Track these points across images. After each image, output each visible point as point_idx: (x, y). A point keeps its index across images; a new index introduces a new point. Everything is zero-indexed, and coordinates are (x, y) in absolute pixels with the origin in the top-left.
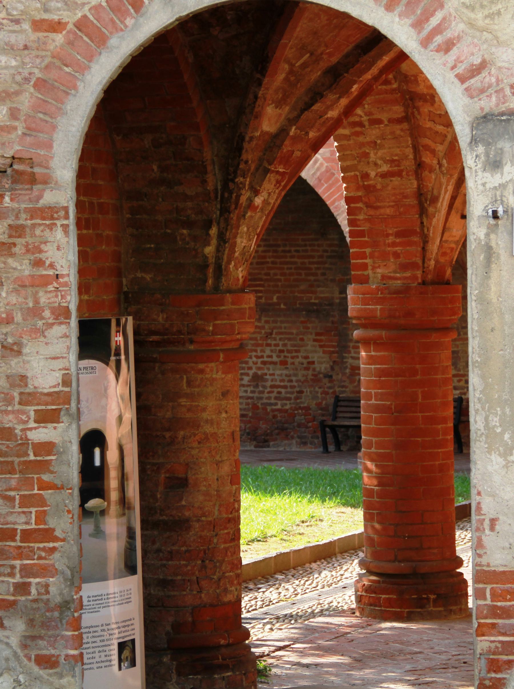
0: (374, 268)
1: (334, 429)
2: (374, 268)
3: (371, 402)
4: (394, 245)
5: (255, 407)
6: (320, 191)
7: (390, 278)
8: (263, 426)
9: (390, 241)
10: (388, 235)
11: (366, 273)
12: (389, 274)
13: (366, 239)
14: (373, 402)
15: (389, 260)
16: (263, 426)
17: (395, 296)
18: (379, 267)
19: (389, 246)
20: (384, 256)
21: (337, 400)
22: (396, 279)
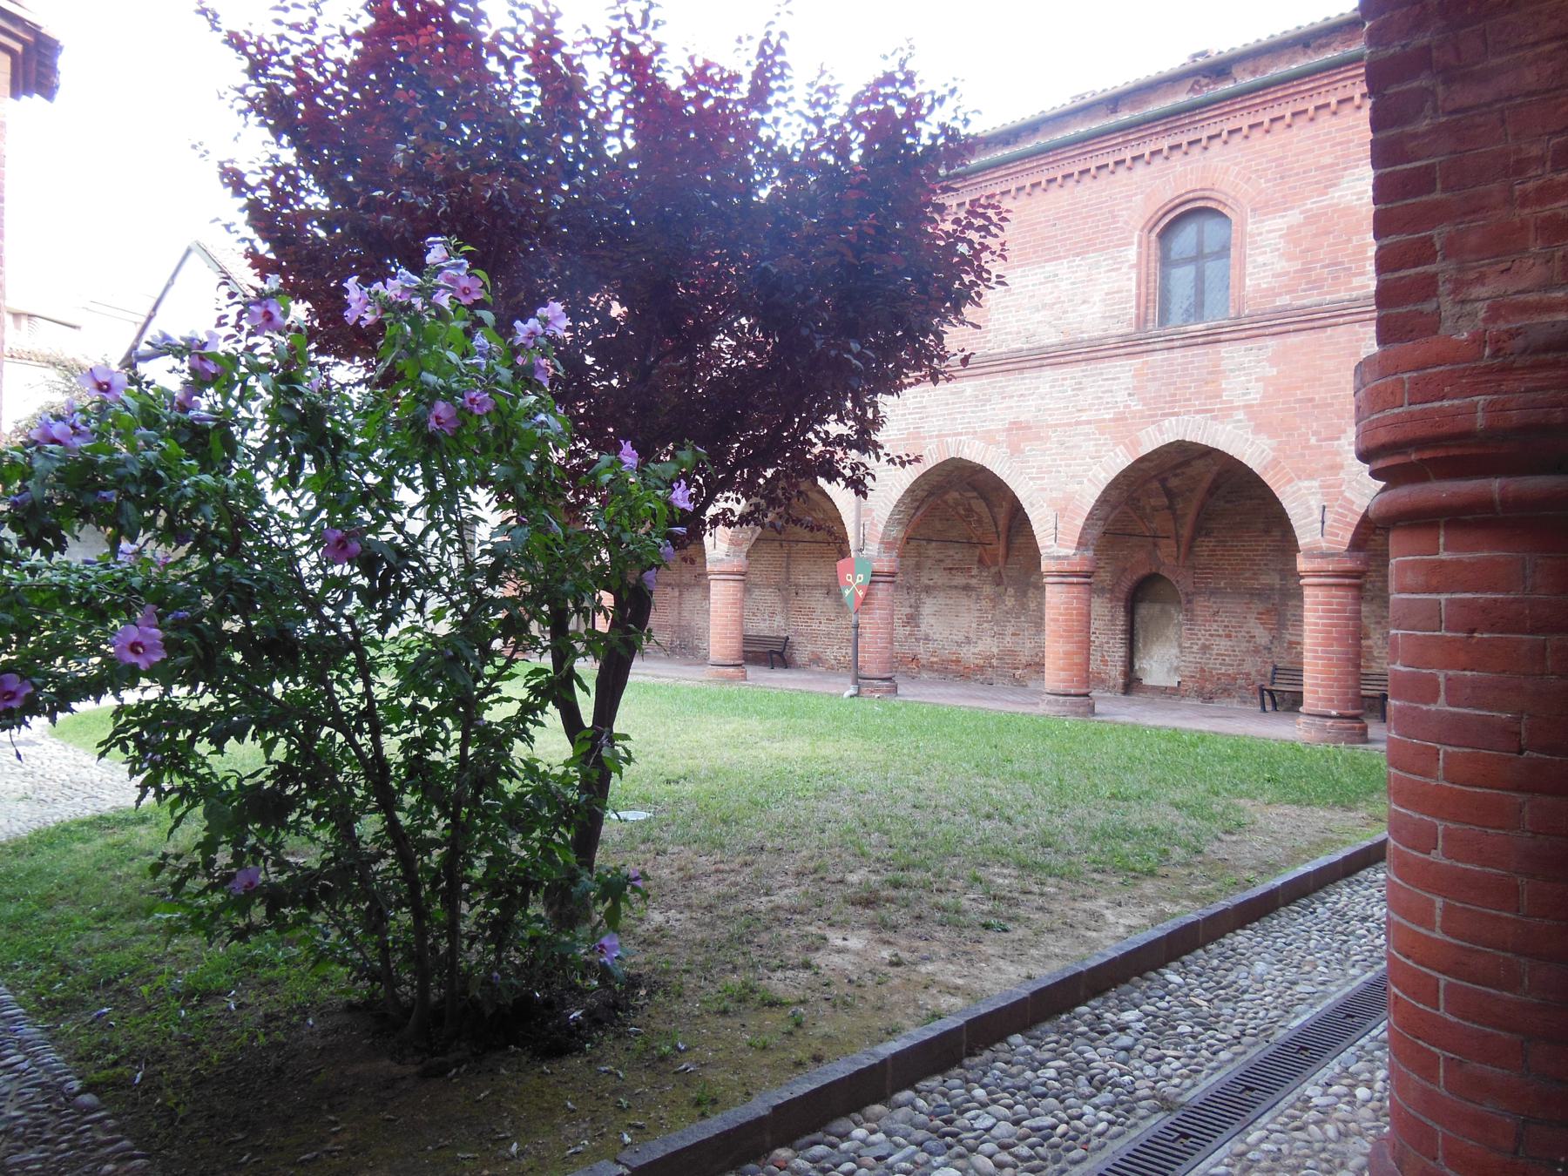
0: (1459, 285)
1: (1271, 692)
2: (1459, 285)
3: (1433, 707)
4: (1546, 193)
5: (1202, 670)
6: (1265, 479)
7: (1525, 308)
8: (1209, 686)
9: (1531, 185)
10: (1520, 168)
11: (1428, 307)
12: (1521, 297)
13: (1437, 195)
14: (1441, 705)
15: (1526, 249)
16: (1209, 686)
17: (1550, 356)
18: (1481, 279)
19: (1525, 201)
20: (1504, 245)
21: (1276, 668)
22: (1551, 308)
